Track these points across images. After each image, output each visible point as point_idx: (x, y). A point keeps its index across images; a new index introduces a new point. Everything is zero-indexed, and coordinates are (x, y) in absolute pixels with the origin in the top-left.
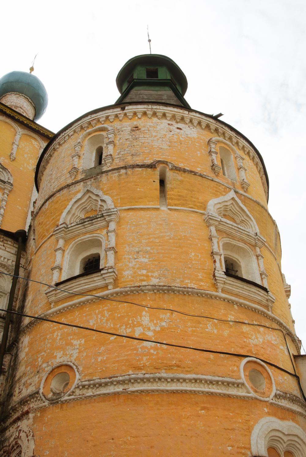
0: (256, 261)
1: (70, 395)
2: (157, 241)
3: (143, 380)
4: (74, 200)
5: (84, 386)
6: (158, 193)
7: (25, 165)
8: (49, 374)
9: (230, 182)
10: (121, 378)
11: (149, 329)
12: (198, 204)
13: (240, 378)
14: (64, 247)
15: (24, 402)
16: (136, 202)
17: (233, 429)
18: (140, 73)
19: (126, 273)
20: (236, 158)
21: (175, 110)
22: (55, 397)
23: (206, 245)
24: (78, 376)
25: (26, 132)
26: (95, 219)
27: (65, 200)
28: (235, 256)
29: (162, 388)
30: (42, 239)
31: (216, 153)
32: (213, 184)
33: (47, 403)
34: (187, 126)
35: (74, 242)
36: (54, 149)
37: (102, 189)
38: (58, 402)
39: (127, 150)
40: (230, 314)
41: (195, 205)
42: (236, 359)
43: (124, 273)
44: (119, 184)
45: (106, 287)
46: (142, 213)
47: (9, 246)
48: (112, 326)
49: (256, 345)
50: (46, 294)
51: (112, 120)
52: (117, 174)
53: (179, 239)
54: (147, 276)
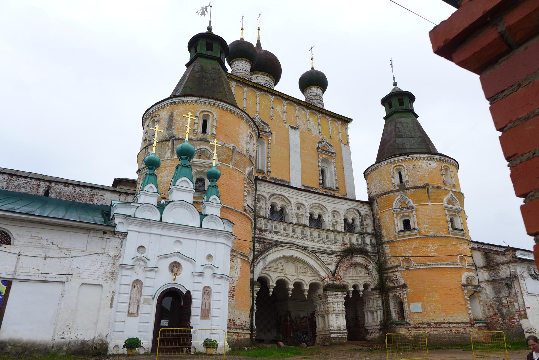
2: (430, 218)
4: (397, 199)
6: (427, 197)
15: (394, 267)
20: (450, 171)
21: (428, 155)
24: (413, 262)
25: (331, 118)
28: (452, 217)
32: (445, 191)
33: (405, 269)
37: (407, 196)
45: (416, 235)
46: (423, 206)
54: (429, 232)
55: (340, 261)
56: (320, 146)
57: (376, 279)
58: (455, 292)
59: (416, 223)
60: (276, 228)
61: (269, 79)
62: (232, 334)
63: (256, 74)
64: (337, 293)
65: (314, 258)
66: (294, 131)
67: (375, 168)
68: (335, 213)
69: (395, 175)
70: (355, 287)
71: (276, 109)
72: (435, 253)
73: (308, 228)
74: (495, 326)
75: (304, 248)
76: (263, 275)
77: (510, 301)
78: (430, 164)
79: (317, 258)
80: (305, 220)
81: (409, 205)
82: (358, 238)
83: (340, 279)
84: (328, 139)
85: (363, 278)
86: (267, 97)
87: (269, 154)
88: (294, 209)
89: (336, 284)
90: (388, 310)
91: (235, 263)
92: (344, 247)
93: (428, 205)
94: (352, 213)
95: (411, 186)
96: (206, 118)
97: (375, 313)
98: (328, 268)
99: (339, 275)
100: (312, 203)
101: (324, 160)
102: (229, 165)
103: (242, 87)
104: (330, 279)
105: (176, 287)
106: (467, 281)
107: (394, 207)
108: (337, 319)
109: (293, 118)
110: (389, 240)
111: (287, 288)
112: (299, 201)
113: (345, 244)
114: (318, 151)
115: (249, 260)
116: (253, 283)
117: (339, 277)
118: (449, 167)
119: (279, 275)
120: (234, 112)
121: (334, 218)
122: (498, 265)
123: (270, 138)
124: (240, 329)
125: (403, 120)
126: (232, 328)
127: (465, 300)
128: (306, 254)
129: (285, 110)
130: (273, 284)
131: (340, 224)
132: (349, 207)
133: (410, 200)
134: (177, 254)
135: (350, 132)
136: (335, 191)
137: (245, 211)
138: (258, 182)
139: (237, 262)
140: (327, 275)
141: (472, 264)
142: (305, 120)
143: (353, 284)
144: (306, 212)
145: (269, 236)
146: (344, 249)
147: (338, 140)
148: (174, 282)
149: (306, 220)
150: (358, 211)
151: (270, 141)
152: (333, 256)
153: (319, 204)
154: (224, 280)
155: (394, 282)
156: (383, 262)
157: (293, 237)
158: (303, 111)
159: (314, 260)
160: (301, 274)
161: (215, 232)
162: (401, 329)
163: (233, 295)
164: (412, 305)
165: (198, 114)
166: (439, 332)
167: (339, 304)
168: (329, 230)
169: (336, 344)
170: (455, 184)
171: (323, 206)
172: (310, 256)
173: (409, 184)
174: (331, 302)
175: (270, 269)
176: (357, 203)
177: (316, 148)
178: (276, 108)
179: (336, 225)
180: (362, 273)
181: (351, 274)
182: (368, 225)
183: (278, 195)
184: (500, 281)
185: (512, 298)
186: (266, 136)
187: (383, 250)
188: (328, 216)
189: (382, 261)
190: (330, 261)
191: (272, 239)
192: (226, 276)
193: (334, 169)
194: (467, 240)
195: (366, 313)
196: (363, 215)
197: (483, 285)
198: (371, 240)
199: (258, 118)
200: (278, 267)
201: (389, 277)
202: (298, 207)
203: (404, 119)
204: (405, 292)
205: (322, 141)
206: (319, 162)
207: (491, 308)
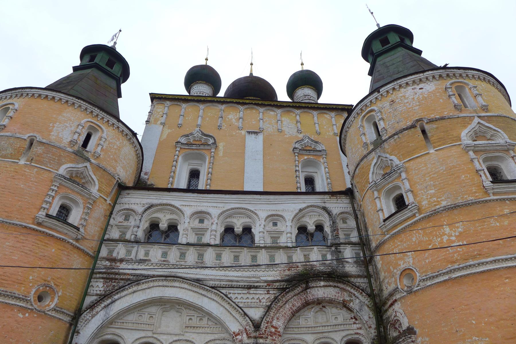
0: (513, 161)
1: (417, 287)
2: (435, 175)
3: (459, 269)
5: (424, 280)
6: (424, 142)
7: (328, 133)
8: (400, 276)
9: (472, 111)
10: (444, 271)
11: (452, 236)
12: (455, 139)
14: (379, 195)
15: (391, 295)
16: (413, 154)
18: (377, 47)
19: (423, 203)
20: (470, 89)
21: (413, 76)
22: (409, 289)
23: (470, 166)
24: (418, 274)
25: (319, 112)
26: (391, 174)
27: (368, 166)
28: (495, 163)
29: (473, 271)
30: (363, 191)
31: (454, 95)
32: (460, 120)
33: (405, 294)
34: (426, 84)
35: (383, 191)
36: (346, 131)
37: (388, 153)
38: (412, 292)
39: (393, 120)
40: (505, 209)
41: (453, 140)
43: (422, 204)
44: (397, 146)
45: (414, 215)
46: (419, 160)
47: (345, 200)
48: (427, 239)
50: (380, 228)
51: (374, 103)
52: (393, 140)
53: (450, 169)
54: (438, 201)
55: (276, 298)
56: (297, 146)
57: (370, 327)
60: (147, 254)
66: (253, 136)
69: (366, 130)
71: (228, 118)
72: (459, 241)
73: (210, 248)
75: (198, 282)
76: (109, 337)
79: (223, 298)
82: (325, 253)
84: (313, 136)
85: (342, 328)
86: (216, 108)
87: (210, 170)
92: (287, 273)
93: (428, 153)
98: (245, 314)
99: (272, 326)
100: (225, 209)
101: (307, 164)
104: (247, 334)
107: (371, 181)
109: (253, 122)
112: (199, 209)
115: (32, 305)
117: (273, 330)
119: (142, 334)
120: (54, 98)
121: (276, 228)
123: (214, 151)
128: (201, 291)
132: (303, 206)
133: (392, 157)
137: (39, 224)
140: (241, 328)
142: (274, 121)
145: (125, 268)
147: (331, 134)
149: (211, 236)
150: (325, 209)
151: (213, 153)
152: (259, 291)
153: (242, 209)
158: (272, 113)
159: (215, 301)
160: (191, 330)
170: (484, 104)
171: (251, 211)
172: (209, 295)
175: (125, 324)
176: (322, 197)
178: (229, 117)
179: (279, 238)
181: (311, 323)
183: (161, 205)
186: (208, 149)
188: (259, 225)
190: (253, 301)
193: (325, 171)
196: (336, 214)
202: (202, 218)
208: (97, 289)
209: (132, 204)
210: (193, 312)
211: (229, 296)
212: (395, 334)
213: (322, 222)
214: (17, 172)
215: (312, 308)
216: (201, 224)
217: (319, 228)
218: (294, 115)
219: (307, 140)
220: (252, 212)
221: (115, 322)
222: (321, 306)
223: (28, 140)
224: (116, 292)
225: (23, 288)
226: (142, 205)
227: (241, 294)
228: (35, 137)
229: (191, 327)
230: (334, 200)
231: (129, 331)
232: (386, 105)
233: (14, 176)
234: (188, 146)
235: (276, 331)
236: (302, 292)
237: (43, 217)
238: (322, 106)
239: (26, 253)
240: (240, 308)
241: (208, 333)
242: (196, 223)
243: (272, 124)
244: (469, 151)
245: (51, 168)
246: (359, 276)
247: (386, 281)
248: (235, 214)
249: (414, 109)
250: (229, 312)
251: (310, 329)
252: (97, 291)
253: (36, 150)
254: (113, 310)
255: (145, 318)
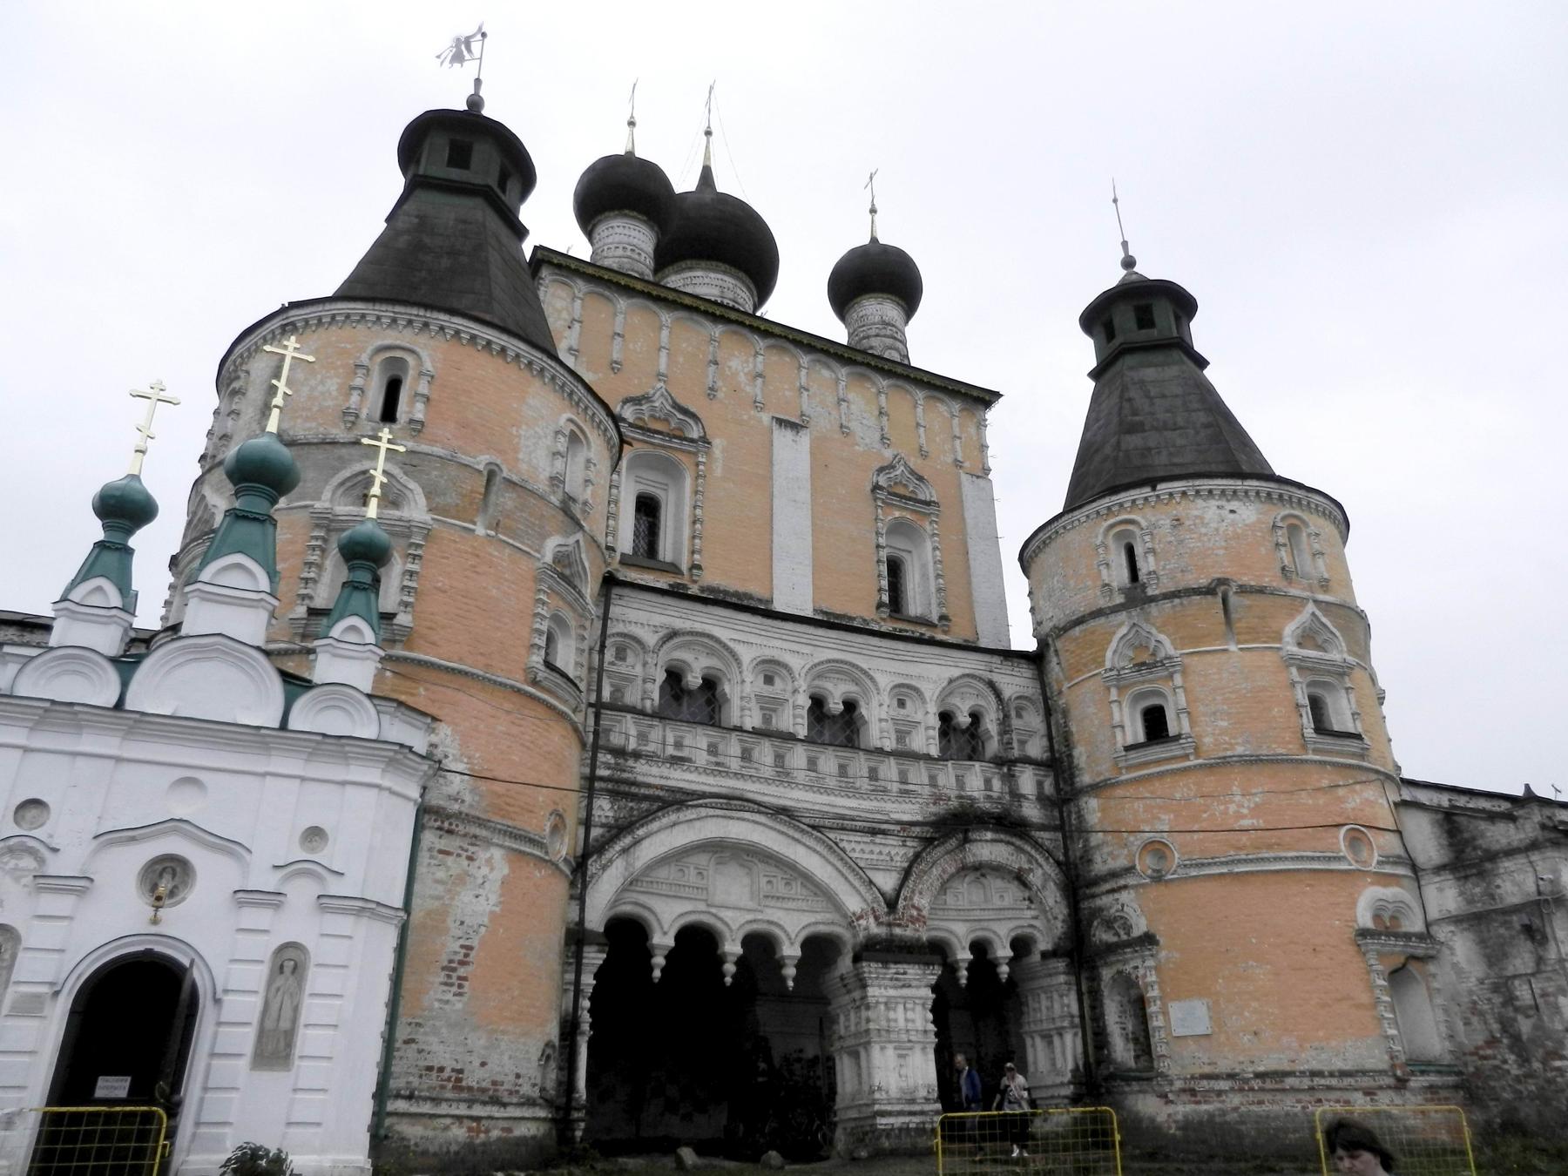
3: (1246, 861)
5: (1185, 866)
6: (1223, 627)
7: (942, 457)
13: (1341, 851)
15: (1114, 875)
17: (1338, 904)
19: (1208, 740)
20: (1309, 535)
21: (1224, 482)
22: (1155, 875)
24: (1177, 855)
28: (1319, 692)
33: (1148, 880)
34: (1241, 503)
37: (1153, 625)
41: (1269, 637)
42: (1335, 829)
45: (1186, 757)
46: (1209, 658)
49: (1353, 809)
51: (1140, 507)
52: (1169, 605)
54: (1231, 744)
55: (917, 856)
56: (882, 481)
57: (1056, 918)
58: (1331, 959)
59: (1184, 717)
60: (678, 745)
61: (733, 282)
62: (448, 1121)
63: (691, 269)
64: (901, 968)
65: (819, 848)
66: (789, 434)
67: (1050, 537)
68: (904, 694)
70: (980, 948)
71: (730, 367)
72: (1252, 818)
73: (799, 744)
74: (1492, 1083)
75: (782, 813)
76: (627, 909)
77: (1542, 989)
78: (1232, 511)
79: (831, 848)
80: (795, 720)
81: (1161, 655)
82: (989, 775)
83: (920, 919)
84: (912, 459)
87: (698, 512)
88: (748, 680)
89: (901, 939)
90: (1098, 1027)
91: (477, 863)
92: (933, 809)
94: (971, 691)
95: (1164, 591)
96: (400, 373)
97: (1056, 1040)
98: (871, 882)
99: (913, 906)
100: (816, 661)
101: (898, 528)
102: (471, 526)
103: (608, 298)
104: (876, 918)
105: (157, 948)
106: (1377, 917)
108: (902, 1061)
109: (787, 393)
110: (1098, 780)
111: (777, 956)
112: (769, 653)
113: (937, 799)
114: (875, 499)
115: (547, 853)
116: (577, 938)
117: (915, 913)
118: (1303, 522)
119: (688, 906)
121: (902, 711)
122: (1493, 856)
123: (704, 460)
124: (484, 1103)
125: (1150, 373)
126: (447, 1100)
127: (1371, 987)
128: (791, 832)
129: (760, 368)
130: (663, 939)
131: (921, 729)
132: (956, 672)
133: (1162, 637)
134: (176, 825)
135: (992, 436)
136: (935, 626)
137: (535, 683)
138: (616, 591)
139: (489, 861)
141: (1399, 857)
143: (972, 936)
144: (795, 691)
145: (650, 774)
146: (935, 815)
147: (950, 460)
148: (154, 929)
149: (795, 716)
150: (991, 685)
151: (701, 467)
152: (891, 841)
154: (365, 921)
155: (1116, 926)
156: (1081, 858)
157: (743, 775)
158: (826, 373)
159: (817, 852)
160: (773, 903)
161: (343, 745)
162: (1141, 1096)
163: (460, 978)
164: (1175, 1009)
165: (364, 359)
166: (1276, 1108)
167: (913, 1010)
168: (880, 751)
169: (894, 1153)
170: (1326, 576)
172: (805, 839)
173: (1157, 584)
174: (880, 1000)
175: (655, 886)
176: (987, 658)
177: (869, 487)
178: (731, 364)
179: (909, 733)
180: (1006, 899)
181: (963, 903)
182: (1031, 733)
183: (691, 633)
184: (1501, 918)
185: (1550, 979)
186: (689, 452)
187: (1080, 817)
189: (1078, 854)
190: (882, 857)
191: (663, 782)
192: (374, 906)
193: (934, 557)
194: (1377, 772)
195: (1029, 1042)
196: (1010, 699)
197: (1442, 933)
198: (1040, 784)
199: (662, 395)
200: (686, 878)
201: (1101, 909)
203: (1153, 373)
204: (1150, 963)
205: (892, 467)
206: (878, 533)
207: (1475, 1020)
208: (602, 813)
209: (630, 622)
210: (774, 869)
211: (841, 845)
212: (1108, 937)
213: (982, 709)
214: (478, 556)
215: (966, 876)
216: (766, 687)
217: (976, 717)
218: (874, 390)
219: (902, 468)
220: (865, 673)
221: (637, 881)
222: (978, 874)
223: (485, 473)
224: (641, 822)
225: (535, 821)
226: (652, 628)
227: (859, 842)
228: (497, 465)
229: (773, 897)
230: (1007, 667)
231: (664, 898)
232: (1162, 522)
233: (475, 567)
234: (643, 435)
235: (919, 915)
236: (957, 848)
237: (543, 668)
238: (938, 383)
239: (528, 748)
240: (861, 868)
241: (804, 911)
242: (760, 687)
243: (827, 406)
244: (1292, 665)
245: (530, 547)
246: (1043, 828)
247: (1106, 850)
248: (831, 671)
249: (1216, 555)
250: (843, 875)
251: (962, 913)
252: (599, 816)
253: (502, 500)
254: (638, 858)
255: (691, 877)
